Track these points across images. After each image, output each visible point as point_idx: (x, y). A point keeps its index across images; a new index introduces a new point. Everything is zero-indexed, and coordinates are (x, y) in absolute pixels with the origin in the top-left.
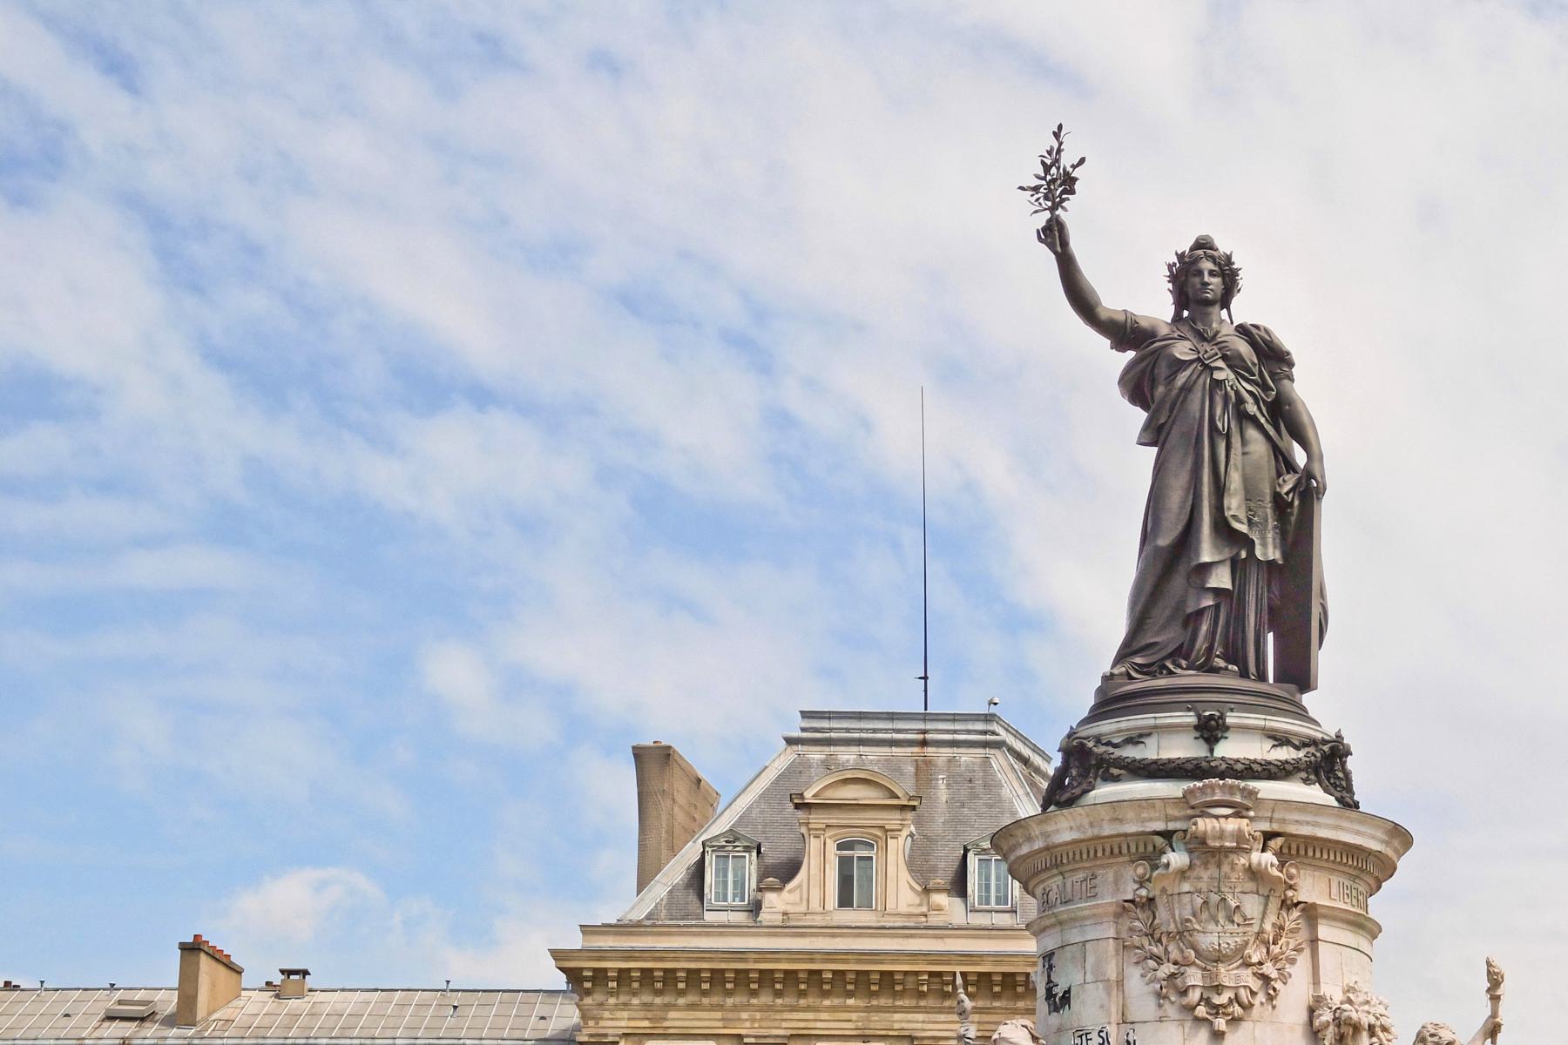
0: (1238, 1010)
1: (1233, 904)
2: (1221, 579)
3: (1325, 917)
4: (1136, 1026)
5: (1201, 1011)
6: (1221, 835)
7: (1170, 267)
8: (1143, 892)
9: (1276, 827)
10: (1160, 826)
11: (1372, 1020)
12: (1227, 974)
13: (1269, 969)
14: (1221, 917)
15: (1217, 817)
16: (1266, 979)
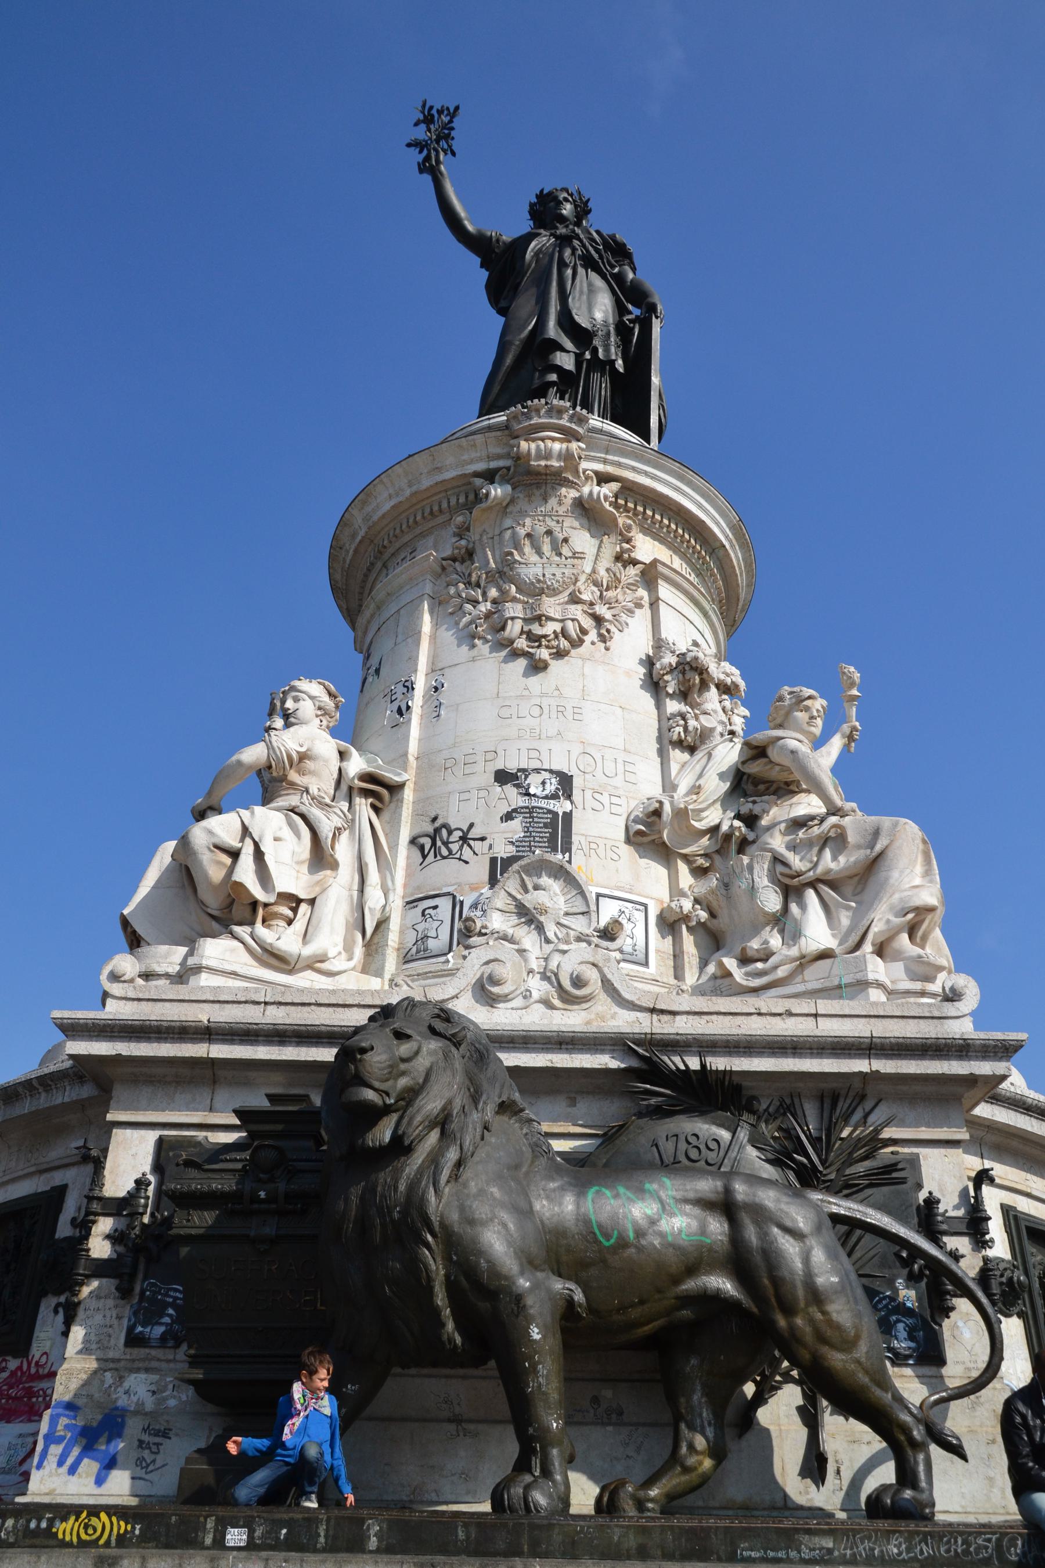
0: (564, 643)
1: (561, 537)
2: (566, 361)
3: (668, 580)
4: (446, 671)
5: (522, 643)
6: (548, 456)
7: (532, 205)
8: (463, 542)
9: (610, 469)
10: (481, 466)
11: (722, 677)
12: (551, 606)
13: (601, 610)
14: (546, 548)
15: (543, 440)
16: (598, 620)
